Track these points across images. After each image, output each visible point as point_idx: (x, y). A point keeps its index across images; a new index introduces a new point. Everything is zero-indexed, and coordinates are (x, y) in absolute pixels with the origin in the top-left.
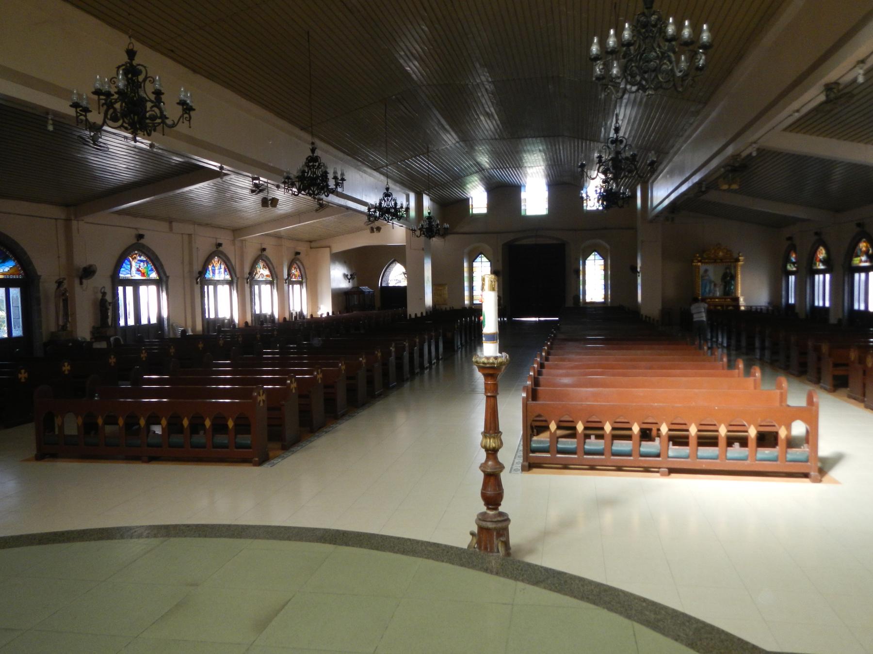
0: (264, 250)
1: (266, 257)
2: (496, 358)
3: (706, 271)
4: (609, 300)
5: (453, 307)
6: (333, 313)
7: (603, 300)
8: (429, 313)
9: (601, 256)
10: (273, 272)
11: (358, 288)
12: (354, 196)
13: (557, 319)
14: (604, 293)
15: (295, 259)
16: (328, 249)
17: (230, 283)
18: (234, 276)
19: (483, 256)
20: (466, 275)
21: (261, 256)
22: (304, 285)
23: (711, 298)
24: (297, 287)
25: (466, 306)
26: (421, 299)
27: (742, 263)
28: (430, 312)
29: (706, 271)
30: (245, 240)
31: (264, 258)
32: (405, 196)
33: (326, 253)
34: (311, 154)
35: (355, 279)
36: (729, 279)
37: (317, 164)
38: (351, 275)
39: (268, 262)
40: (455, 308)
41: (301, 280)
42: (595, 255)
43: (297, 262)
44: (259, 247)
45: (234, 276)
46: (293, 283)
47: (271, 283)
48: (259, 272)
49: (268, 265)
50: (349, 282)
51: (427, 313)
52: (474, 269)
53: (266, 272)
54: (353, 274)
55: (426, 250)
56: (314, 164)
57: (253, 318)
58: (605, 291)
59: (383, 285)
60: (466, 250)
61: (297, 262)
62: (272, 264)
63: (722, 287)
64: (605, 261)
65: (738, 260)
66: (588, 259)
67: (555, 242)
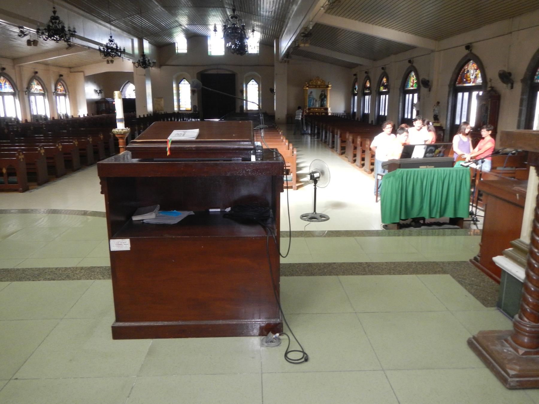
0: (36, 73)
1: (39, 78)
2: (122, 130)
3: (311, 92)
5: (166, 112)
6: (88, 115)
7: (258, 109)
8: (149, 115)
10: (44, 88)
11: (104, 99)
12: (93, 39)
15: (60, 79)
16: (82, 73)
17: (14, 94)
18: (16, 89)
20: (175, 92)
21: (35, 76)
22: (67, 96)
23: (313, 108)
24: (62, 98)
27: (330, 88)
28: (150, 114)
29: (311, 92)
30: (22, 66)
31: (37, 79)
32: (130, 40)
33: (81, 76)
34: (53, 15)
35: (103, 93)
36: (323, 97)
37: (58, 21)
38: (100, 91)
39: (40, 81)
40: (168, 112)
41: (65, 93)
43: (61, 81)
44: (33, 70)
45: (16, 89)
46: (60, 95)
47: (43, 95)
48: (34, 87)
49: (40, 83)
50: (99, 95)
53: (39, 87)
55: (147, 75)
56: (56, 21)
57: (32, 118)
60: (174, 76)
61: (61, 81)
62: (42, 82)
63: (320, 102)
65: (328, 87)
67: (227, 73)
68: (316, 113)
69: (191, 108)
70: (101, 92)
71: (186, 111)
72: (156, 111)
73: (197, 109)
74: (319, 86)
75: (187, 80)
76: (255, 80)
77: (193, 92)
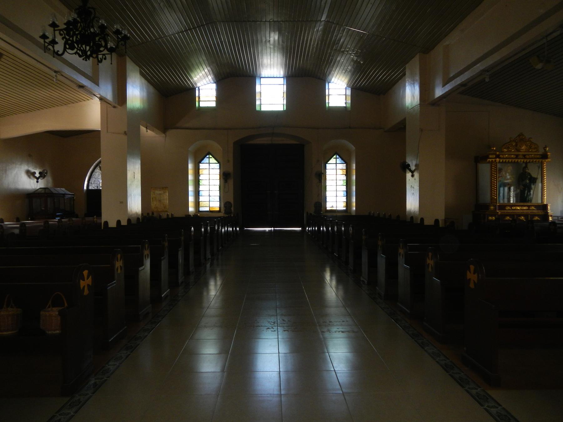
4: (354, 209)
7: (345, 208)
9: (342, 159)
13: (300, 229)
14: (345, 200)
19: (210, 156)
20: (191, 177)
25: (190, 214)
26: (121, 203)
28: (138, 219)
38: (40, 173)
40: (176, 215)
42: (336, 158)
50: (37, 182)
51: (129, 220)
52: (200, 171)
54: (44, 170)
58: (347, 198)
59: (90, 188)
60: (191, 148)
68: (520, 215)
69: (220, 208)
70: (42, 175)
71: (211, 213)
72: (153, 213)
73: (232, 209)
74: (524, 156)
76: (339, 156)
77: (225, 176)
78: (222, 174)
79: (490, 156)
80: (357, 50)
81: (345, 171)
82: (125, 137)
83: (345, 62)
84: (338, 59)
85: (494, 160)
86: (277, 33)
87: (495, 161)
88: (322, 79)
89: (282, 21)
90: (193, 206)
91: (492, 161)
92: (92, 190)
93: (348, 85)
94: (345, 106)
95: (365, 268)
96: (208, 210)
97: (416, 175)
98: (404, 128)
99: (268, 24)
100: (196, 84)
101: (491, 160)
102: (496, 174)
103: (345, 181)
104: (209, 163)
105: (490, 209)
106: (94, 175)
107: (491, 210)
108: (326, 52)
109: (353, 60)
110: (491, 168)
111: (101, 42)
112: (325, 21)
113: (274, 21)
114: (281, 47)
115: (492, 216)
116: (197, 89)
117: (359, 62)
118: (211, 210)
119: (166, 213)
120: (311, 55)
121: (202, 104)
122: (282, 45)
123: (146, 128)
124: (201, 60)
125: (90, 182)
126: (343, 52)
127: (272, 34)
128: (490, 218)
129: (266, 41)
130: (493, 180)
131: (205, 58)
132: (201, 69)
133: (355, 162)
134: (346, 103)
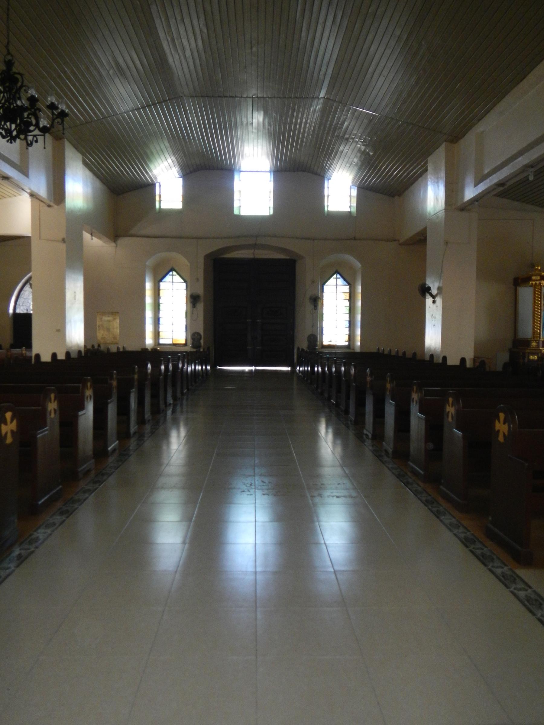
4: (359, 343)
5: (124, 348)
7: (347, 343)
9: (345, 279)
13: (289, 369)
14: (348, 333)
19: (175, 273)
20: (149, 300)
25: (147, 347)
26: (58, 331)
28: (80, 352)
42: (337, 278)
51: (68, 354)
58: (350, 331)
59: (18, 311)
60: (150, 262)
64: (350, 289)
66: (326, 284)
69: (186, 340)
72: (99, 346)
73: (202, 341)
75: (178, 274)
76: (341, 275)
78: (189, 296)
79: (534, 278)
80: (366, 137)
81: (348, 295)
82: (63, 247)
83: (350, 152)
84: (341, 148)
85: (538, 282)
86: (262, 113)
87: (540, 283)
88: (319, 175)
89: (269, 97)
90: (152, 337)
91: (536, 283)
92: (20, 314)
93: (354, 184)
94: (349, 210)
95: (369, 419)
96: (171, 342)
97: (439, 300)
98: (425, 240)
99: (250, 101)
100: (156, 178)
101: (534, 283)
102: (540, 301)
103: (348, 308)
104: (173, 282)
105: (532, 345)
106: (22, 294)
107: (533, 347)
108: (326, 139)
109: (359, 150)
110: (535, 293)
111: (30, 118)
112: (324, 98)
113: (257, 97)
114: (267, 131)
115: (533, 354)
116: (157, 185)
117: (368, 153)
118: (175, 342)
119: (116, 346)
120: (306, 143)
121: (165, 205)
122: (269, 128)
123: (91, 234)
124: (163, 146)
125: (18, 303)
126: (347, 139)
127: (256, 114)
128: (531, 357)
129: (247, 123)
130: (537, 308)
131: (167, 144)
132: (163, 158)
133: (360, 284)
134: (350, 207)
